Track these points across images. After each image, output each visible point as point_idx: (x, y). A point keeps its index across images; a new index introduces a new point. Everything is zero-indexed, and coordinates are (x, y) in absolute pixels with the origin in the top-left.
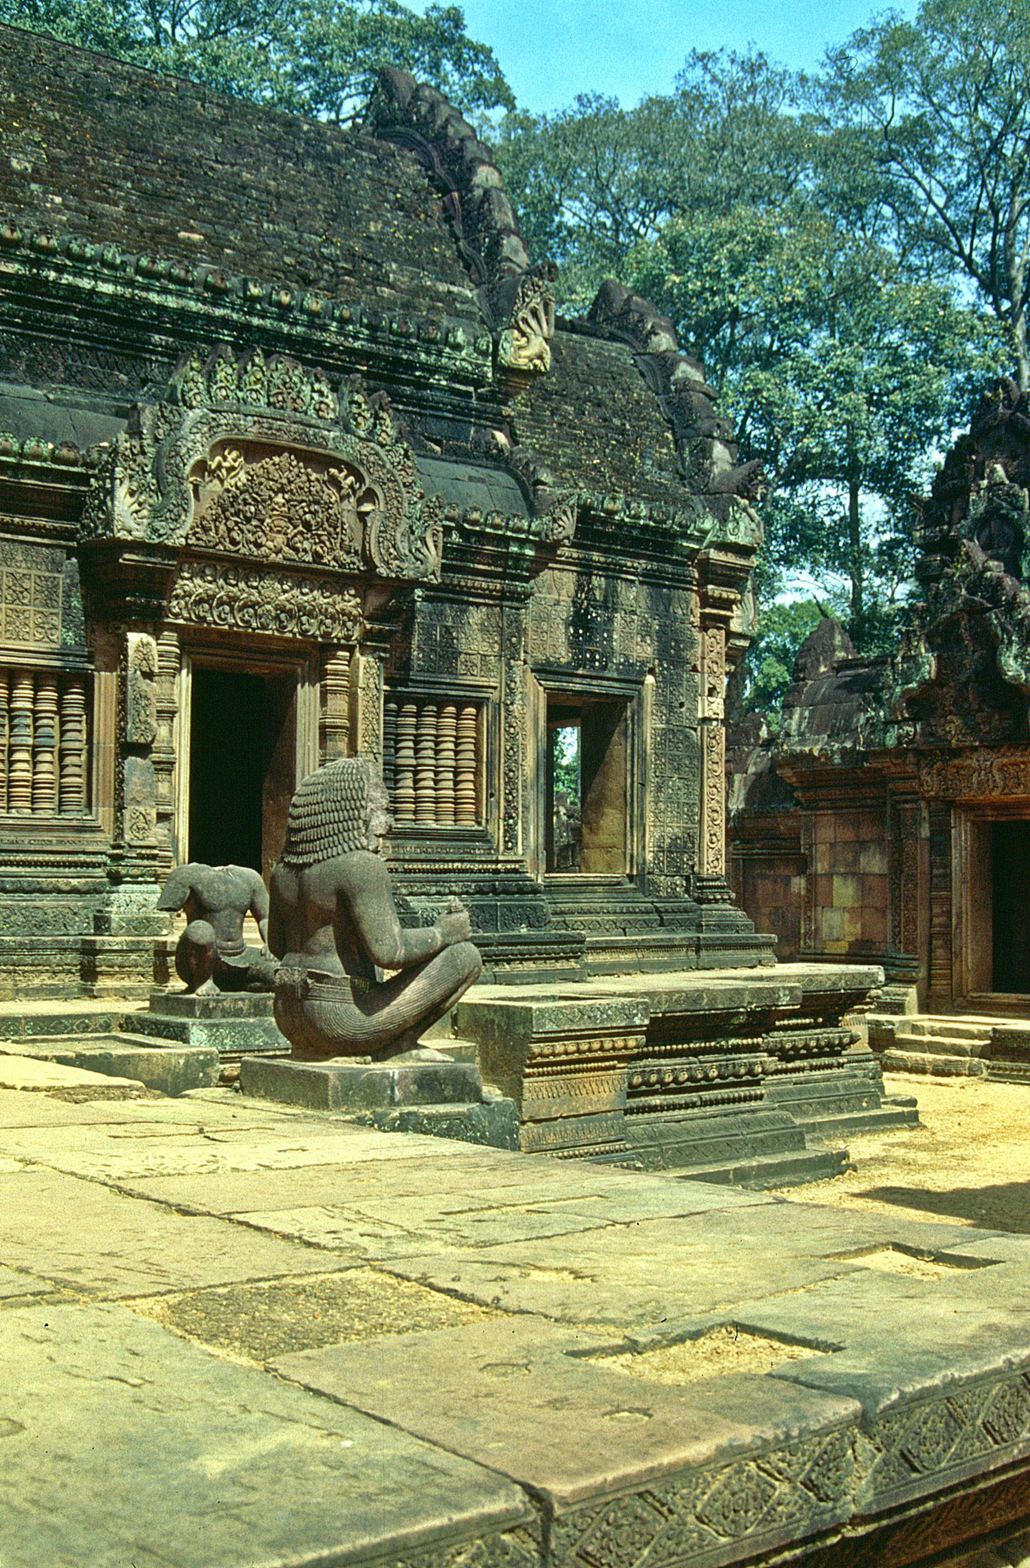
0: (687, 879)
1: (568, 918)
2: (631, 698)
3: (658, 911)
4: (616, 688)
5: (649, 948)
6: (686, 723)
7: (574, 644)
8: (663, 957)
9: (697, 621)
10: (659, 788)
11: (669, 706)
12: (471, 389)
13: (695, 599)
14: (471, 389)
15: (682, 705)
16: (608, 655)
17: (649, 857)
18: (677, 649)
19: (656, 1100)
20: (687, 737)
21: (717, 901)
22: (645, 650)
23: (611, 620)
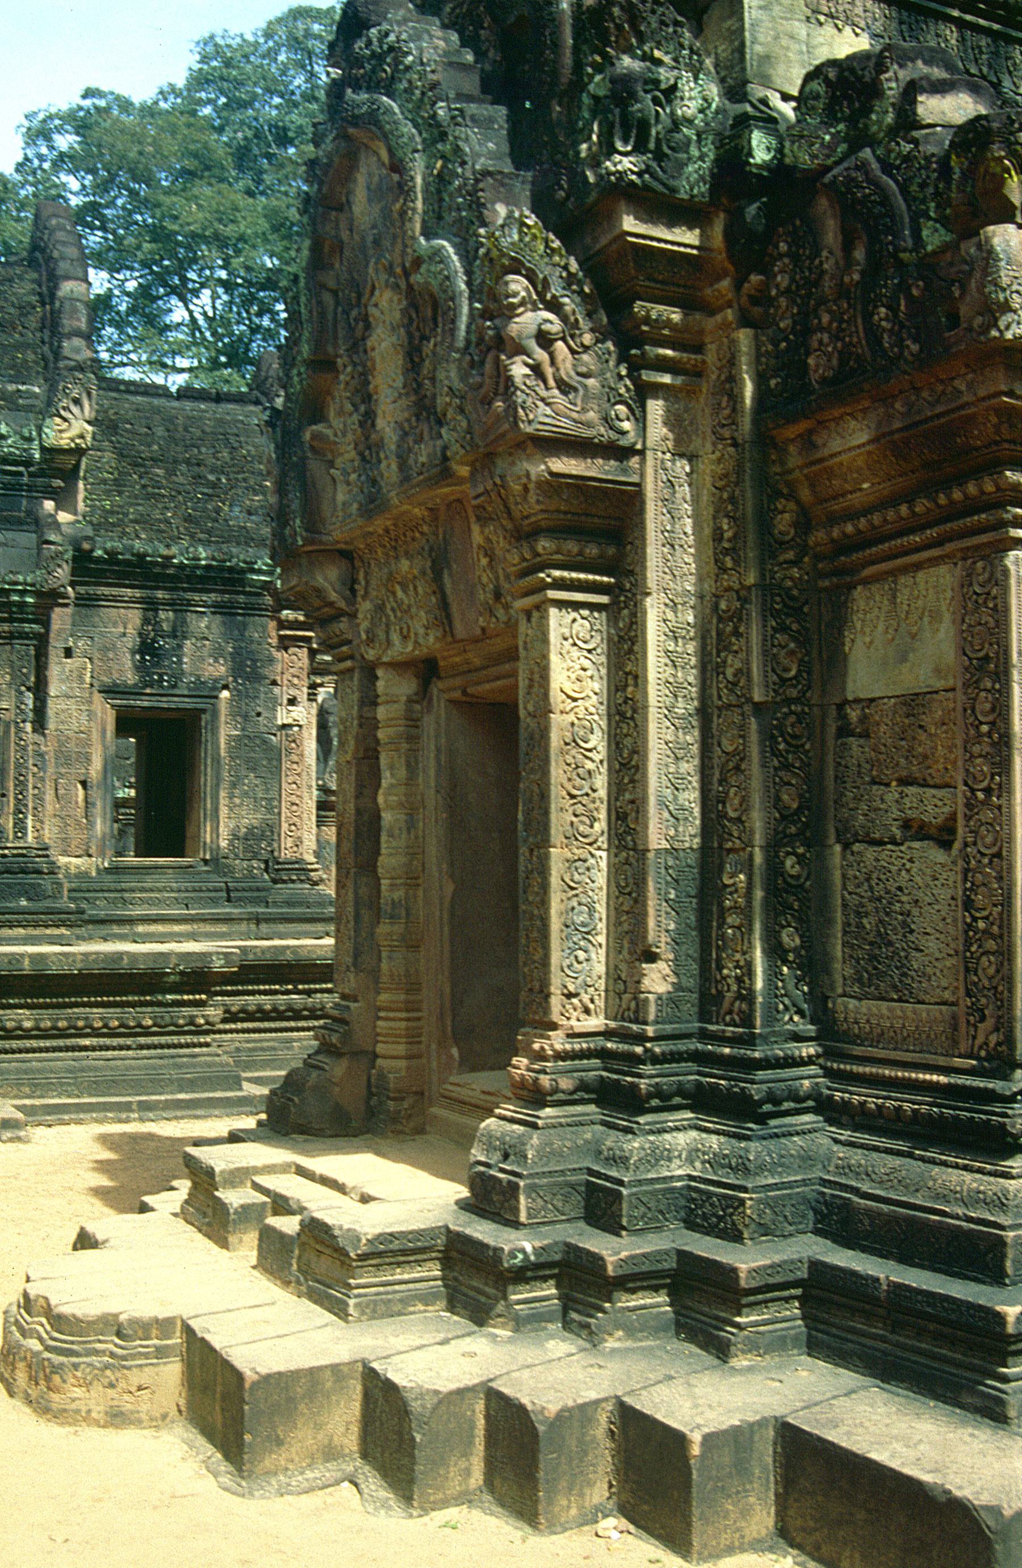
0: (266, 862)
1: (126, 895)
2: (204, 711)
3: (228, 890)
4: (188, 703)
5: (204, 920)
6: (264, 729)
7: (140, 668)
8: (223, 928)
9: (274, 641)
10: (234, 785)
11: (243, 715)
12: (21, 469)
13: (272, 625)
14: (21, 469)
15: (259, 714)
16: (177, 676)
17: (224, 844)
18: (254, 667)
19: (86, 1042)
20: (265, 742)
21: (293, 881)
22: (220, 670)
23: (180, 647)
